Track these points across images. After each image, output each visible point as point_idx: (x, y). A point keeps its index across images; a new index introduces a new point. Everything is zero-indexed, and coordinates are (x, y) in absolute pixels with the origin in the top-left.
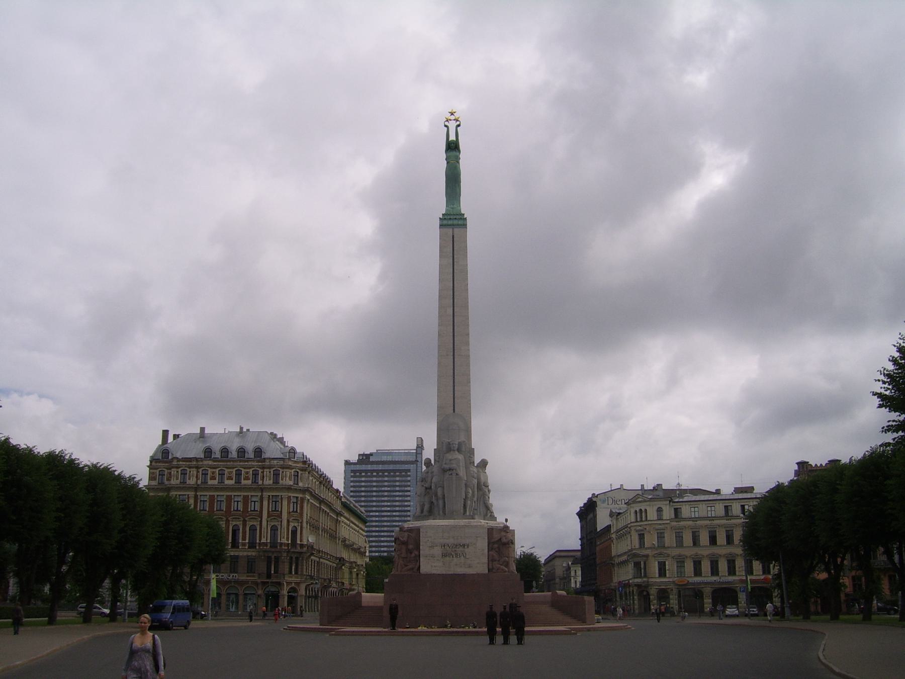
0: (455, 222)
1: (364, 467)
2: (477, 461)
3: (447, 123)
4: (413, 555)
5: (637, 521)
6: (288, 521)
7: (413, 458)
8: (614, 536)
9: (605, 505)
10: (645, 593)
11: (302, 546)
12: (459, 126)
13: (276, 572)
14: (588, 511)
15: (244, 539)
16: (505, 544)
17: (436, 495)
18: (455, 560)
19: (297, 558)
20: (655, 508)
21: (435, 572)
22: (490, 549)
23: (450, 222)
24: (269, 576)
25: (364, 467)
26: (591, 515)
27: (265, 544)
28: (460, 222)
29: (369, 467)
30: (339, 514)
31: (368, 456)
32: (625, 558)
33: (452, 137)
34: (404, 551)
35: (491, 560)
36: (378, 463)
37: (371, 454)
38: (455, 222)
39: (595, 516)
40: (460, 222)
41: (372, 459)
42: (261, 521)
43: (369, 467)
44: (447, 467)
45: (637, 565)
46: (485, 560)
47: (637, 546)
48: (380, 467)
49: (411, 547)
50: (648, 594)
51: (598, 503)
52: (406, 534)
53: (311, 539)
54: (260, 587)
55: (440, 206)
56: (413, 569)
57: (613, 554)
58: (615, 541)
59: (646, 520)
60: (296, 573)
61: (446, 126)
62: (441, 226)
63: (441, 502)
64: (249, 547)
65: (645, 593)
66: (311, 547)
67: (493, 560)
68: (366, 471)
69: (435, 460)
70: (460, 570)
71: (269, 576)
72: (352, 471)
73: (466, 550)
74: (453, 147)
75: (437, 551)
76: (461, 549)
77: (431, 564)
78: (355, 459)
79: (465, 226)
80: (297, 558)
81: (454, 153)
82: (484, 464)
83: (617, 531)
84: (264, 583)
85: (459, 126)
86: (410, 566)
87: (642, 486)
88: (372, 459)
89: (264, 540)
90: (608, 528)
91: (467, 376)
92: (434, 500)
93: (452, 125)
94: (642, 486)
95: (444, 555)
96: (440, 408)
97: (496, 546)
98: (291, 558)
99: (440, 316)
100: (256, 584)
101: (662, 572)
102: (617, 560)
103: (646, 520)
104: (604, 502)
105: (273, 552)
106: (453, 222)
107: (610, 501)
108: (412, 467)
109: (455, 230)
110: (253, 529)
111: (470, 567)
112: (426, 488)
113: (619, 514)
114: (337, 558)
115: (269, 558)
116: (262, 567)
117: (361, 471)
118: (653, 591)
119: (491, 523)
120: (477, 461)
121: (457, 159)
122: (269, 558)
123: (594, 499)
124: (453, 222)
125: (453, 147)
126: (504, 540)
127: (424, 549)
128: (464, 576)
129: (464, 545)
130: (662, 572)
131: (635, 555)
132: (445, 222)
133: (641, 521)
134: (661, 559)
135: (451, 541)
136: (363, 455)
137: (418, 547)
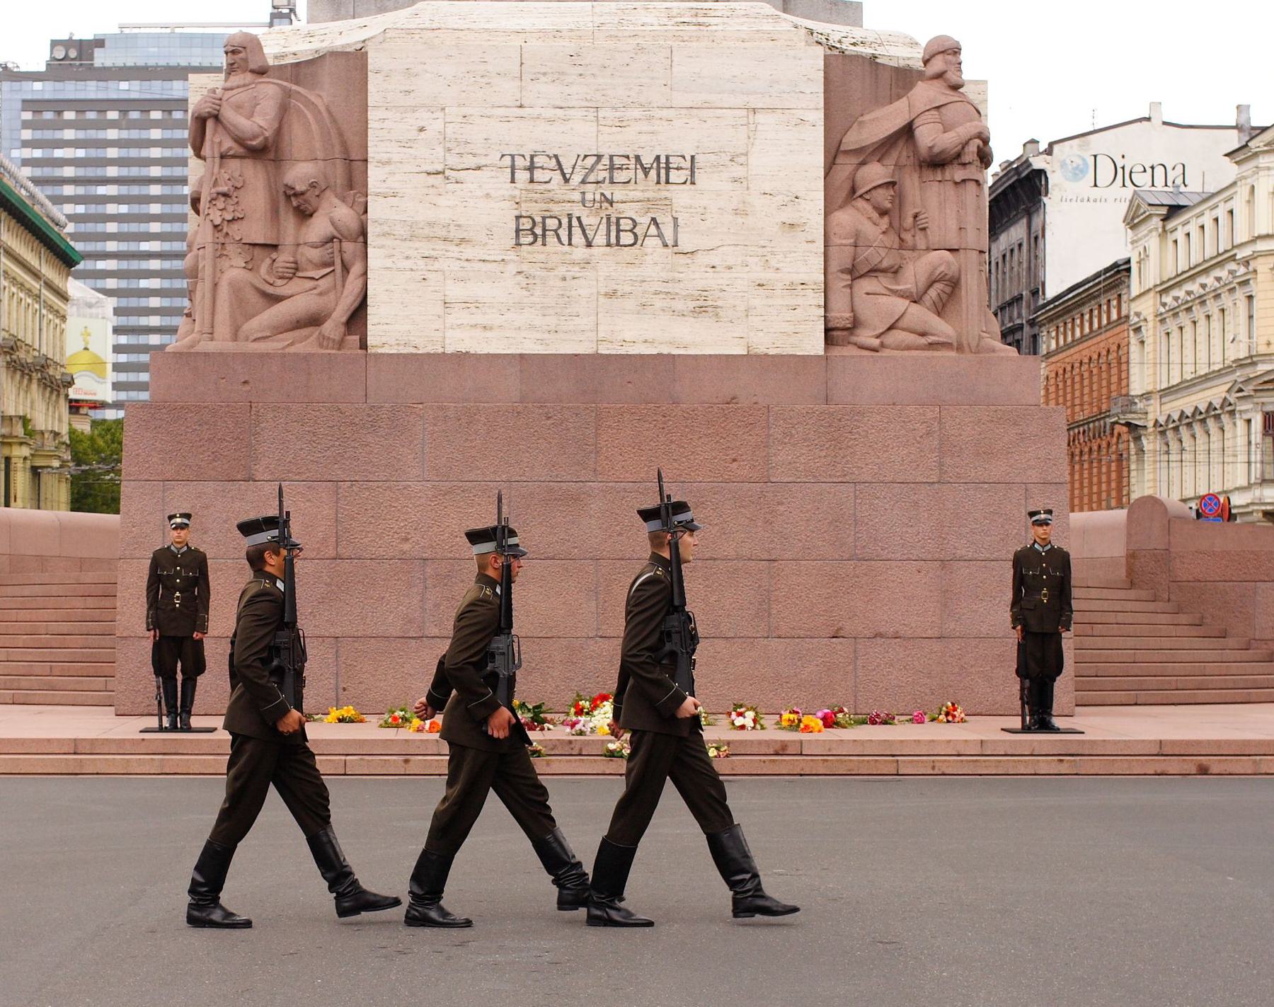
1: (71, 90)
4: (319, 227)
8: (1146, 308)
16: (937, 163)
18: (608, 265)
22: (841, 193)
25: (71, 90)
26: (1017, 232)
29: (92, 90)
31: (85, 48)
32: (1215, 394)
34: (256, 198)
37: (99, 43)
39: (1036, 239)
41: (101, 58)
43: (92, 90)
51: (1053, 179)
52: (269, 91)
56: (314, 320)
57: (1136, 388)
58: (1148, 332)
67: (855, 273)
68: (81, 105)
70: (636, 333)
72: (27, 104)
73: (681, 196)
75: (488, 204)
76: (646, 188)
78: (36, 60)
83: (1164, 289)
86: (300, 300)
88: (101, 58)
90: (1118, 273)
95: (531, 231)
97: (875, 173)
102: (1156, 412)
104: (1078, 173)
111: (703, 308)
113: (1174, 210)
117: (58, 106)
123: (1037, 163)
126: (929, 137)
127: (396, 190)
128: (665, 364)
129: (663, 168)
135: (577, 137)
136: (68, 44)
137: (352, 172)
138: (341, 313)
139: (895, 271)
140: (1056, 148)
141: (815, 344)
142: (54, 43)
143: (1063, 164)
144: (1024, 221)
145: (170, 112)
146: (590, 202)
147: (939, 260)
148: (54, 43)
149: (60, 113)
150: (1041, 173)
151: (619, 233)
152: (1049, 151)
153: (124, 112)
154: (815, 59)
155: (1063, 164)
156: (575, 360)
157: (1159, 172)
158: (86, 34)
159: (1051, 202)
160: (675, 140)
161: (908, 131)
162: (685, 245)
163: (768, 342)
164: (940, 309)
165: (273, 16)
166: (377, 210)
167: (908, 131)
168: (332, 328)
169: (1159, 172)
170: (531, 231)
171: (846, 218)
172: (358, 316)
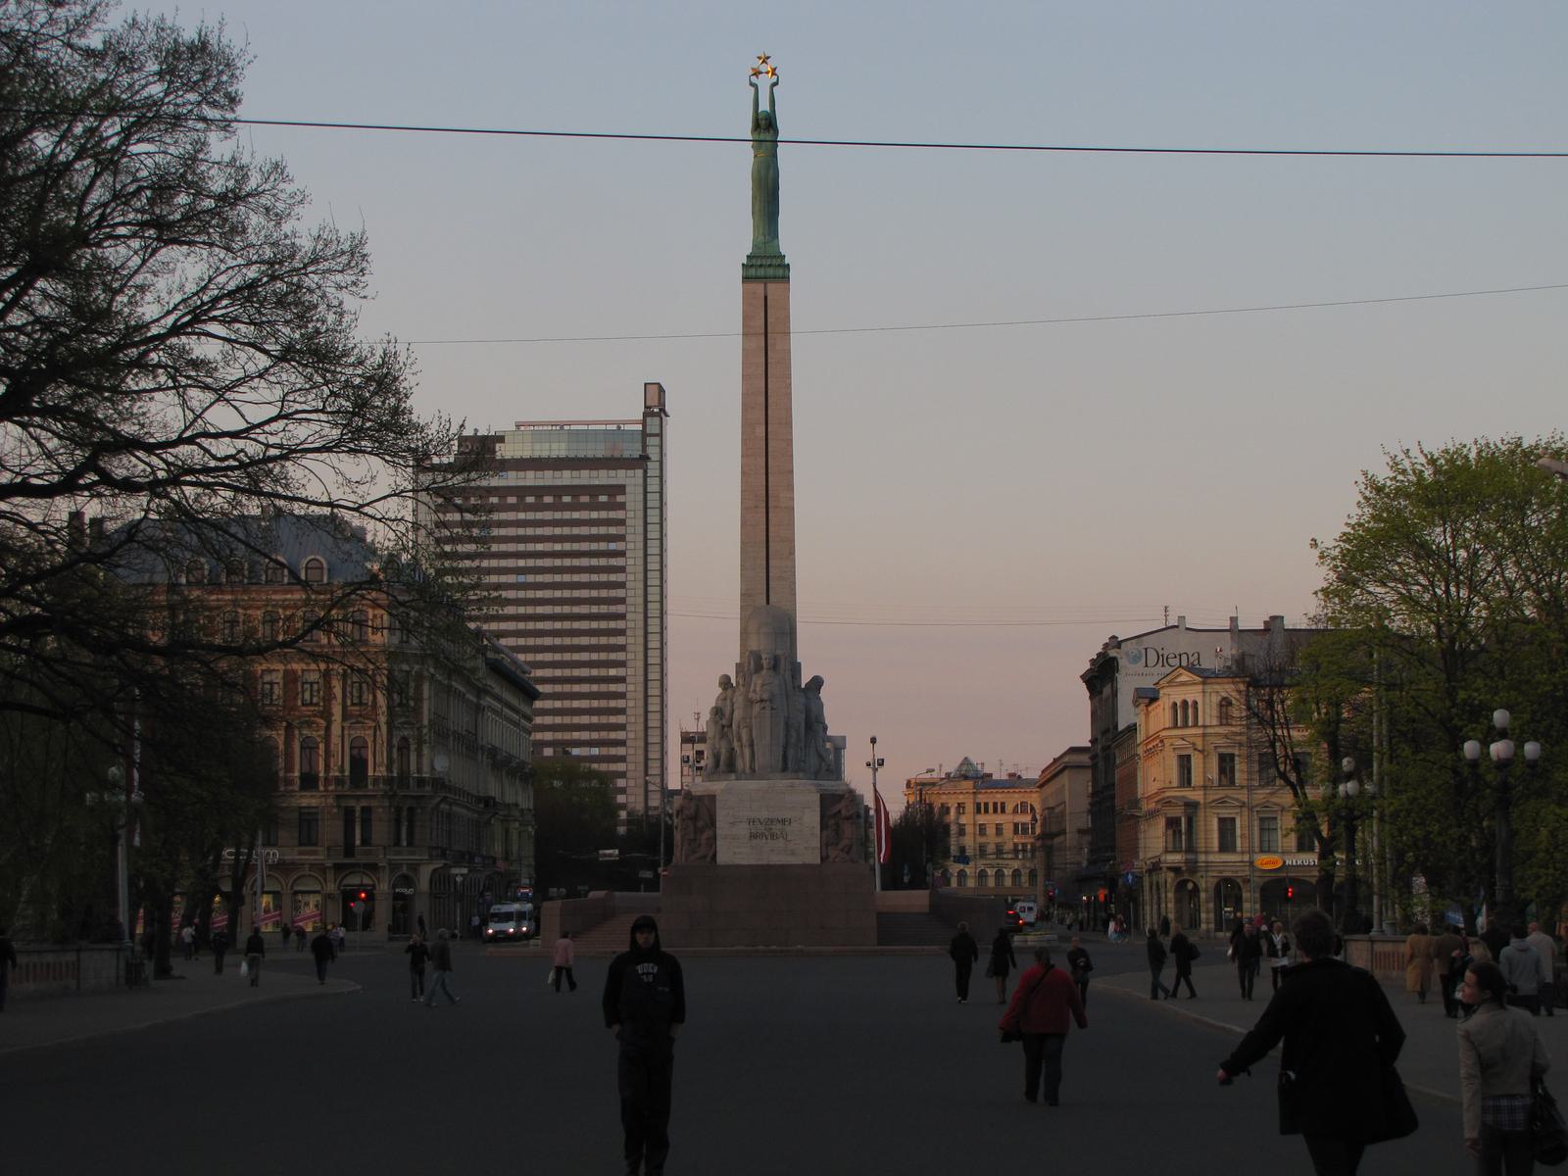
0: (771, 272)
2: (805, 679)
3: (754, 79)
4: (705, 836)
5: (1175, 726)
6: (390, 724)
7: (634, 451)
9: (1140, 666)
10: (1190, 886)
11: (421, 782)
12: (776, 84)
13: (365, 841)
14: (1101, 675)
15: (289, 768)
19: (411, 810)
20: (1215, 699)
21: (738, 861)
23: (761, 272)
24: (349, 850)
27: (339, 781)
28: (780, 272)
30: (482, 691)
35: (825, 845)
37: (501, 439)
38: (771, 272)
39: (1115, 694)
40: (780, 272)
41: (503, 451)
42: (328, 729)
45: (1172, 823)
47: (1175, 783)
48: (530, 478)
49: (700, 824)
50: (1196, 890)
51: (1123, 663)
53: (441, 764)
54: (330, 875)
55: (742, 241)
56: (705, 857)
57: (1140, 791)
59: (1196, 725)
60: (410, 844)
61: (751, 84)
62: (746, 279)
63: (747, 751)
64: (303, 788)
65: (1190, 886)
66: (439, 783)
67: (827, 845)
69: (737, 683)
70: (777, 859)
71: (349, 850)
73: (788, 828)
75: (743, 830)
76: (779, 826)
77: (734, 849)
79: (786, 279)
80: (411, 810)
82: (817, 683)
84: (338, 867)
85: (776, 84)
87: (1234, 620)
88: (503, 451)
89: (335, 773)
91: (790, 542)
93: (763, 83)
94: (1234, 620)
95: (753, 836)
96: (745, 595)
97: (832, 821)
98: (399, 810)
99: (744, 441)
100: (323, 869)
101: (1227, 846)
103: (1196, 725)
104: (1135, 659)
105: (358, 798)
106: (766, 269)
107: (1152, 657)
108: (631, 479)
109: (769, 286)
110: (308, 747)
111: (793, 853)
112: (723, 727)
114: (479, 799)
115: (349, 813)
116: (331, 830)
118: (1206, 883)
119: (829, 785)
120: (805, 679)
122: (349, 813)
123: (1112, 653)
124: (766, 269)
125: (765, 125)
128: (783, 867)
129: (783, 821)
130: (1227, 846)
131: (1168, 802)
132: (752, 272)
133: (1185, 725)
134: (1225, 813)
135: (764, 815)
137: (712, 823)
138: (711, 854)
139: (837, 844)
140: (1123, 645)
141: (818, 861)
143: (1127, 654)
144: (1109, 686)
145: (560, 497)
146: (768, 829)
149: (467, 499)
150: (1114, 659)
151: (773, 836)
154: (817, 798)
155: (1127, 654)
156: (762, 866)
157: (1184, 657)
160: (787, 815)
161: (840, 811)
162: (789, 838)
163: (807, 862)
164: (848, 853)
165: (645, 415)
166: (719, 832)
167: (840, 811)
168: (708, 859)
169: (1184, 657)
170: (753, 836)
171: (825, 832)
172: (714, 856)
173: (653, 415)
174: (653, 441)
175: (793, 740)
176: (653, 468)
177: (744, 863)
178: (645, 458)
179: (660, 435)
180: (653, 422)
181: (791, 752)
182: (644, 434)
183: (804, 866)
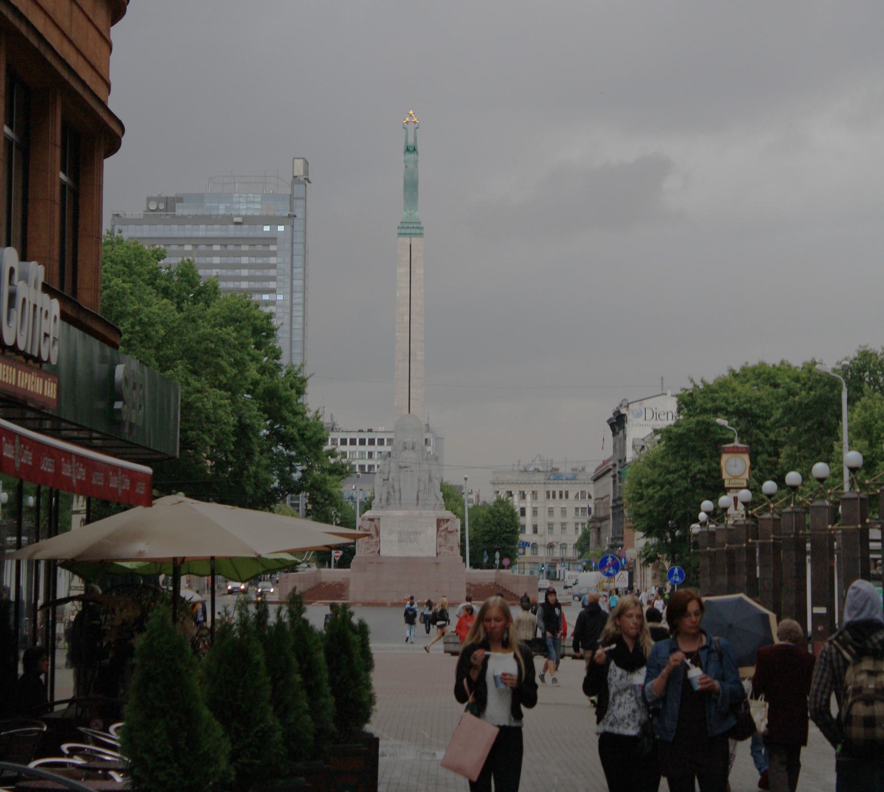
4: (374, 540)
9: (641, 420)
17: (393, 487)
23: (408, 231)
28: (418, 231)
31: (170, 203)
33: (411, 141)
36: (196, 220)
37: (180, 200)
38: (413, 231)
40: (418, 231)
41: (181, 210)
44: (403, 465)
46: (434, 545)
51: (630, 417)
63: (397, 494)
70: (413, 554)
74: (411, 149)
81: (411, 156)
86: (372, 550)
92: (391, 490)
95: (400, 541)
97: (443, 533)
104: (638, 415)
107: (649, 414)
121: (416, 162)
123: (623, 411)
125: (411, 149)
126: (449, 529)
128: (416, 558)
132: (403, 231)
142: (149, 200)
145: (226, 246)
147: (451, 544)
148: (149, 200)
150: (624, 415)
152: (627, 406)
153: (196, 246)
158: (171, 194)
159: (628, 426)
166: (381, 539)
172: (379, 552)
173: (299, 182)
174: (298, 203)
175: (422, 488)
176: (298, 223)
177: (396, 555)
178: (292, 217)
179: (305, 199)
180: (299, 190)
181: (421, 495)
182: (292, 198)
183: (428, 558)
